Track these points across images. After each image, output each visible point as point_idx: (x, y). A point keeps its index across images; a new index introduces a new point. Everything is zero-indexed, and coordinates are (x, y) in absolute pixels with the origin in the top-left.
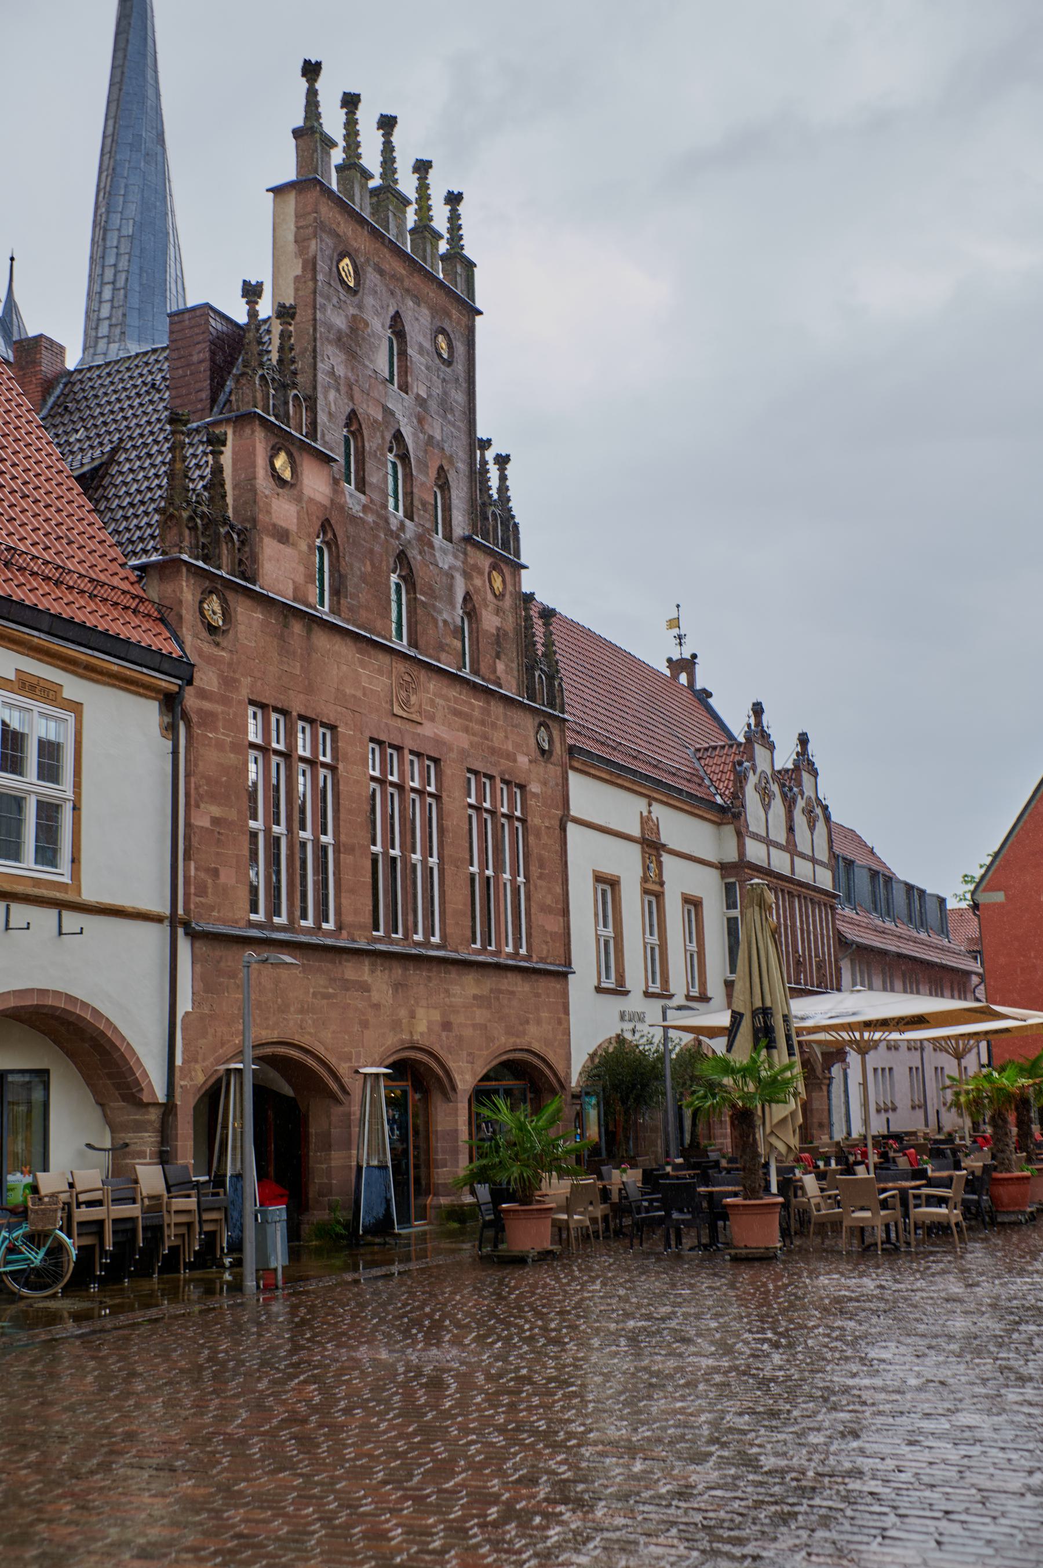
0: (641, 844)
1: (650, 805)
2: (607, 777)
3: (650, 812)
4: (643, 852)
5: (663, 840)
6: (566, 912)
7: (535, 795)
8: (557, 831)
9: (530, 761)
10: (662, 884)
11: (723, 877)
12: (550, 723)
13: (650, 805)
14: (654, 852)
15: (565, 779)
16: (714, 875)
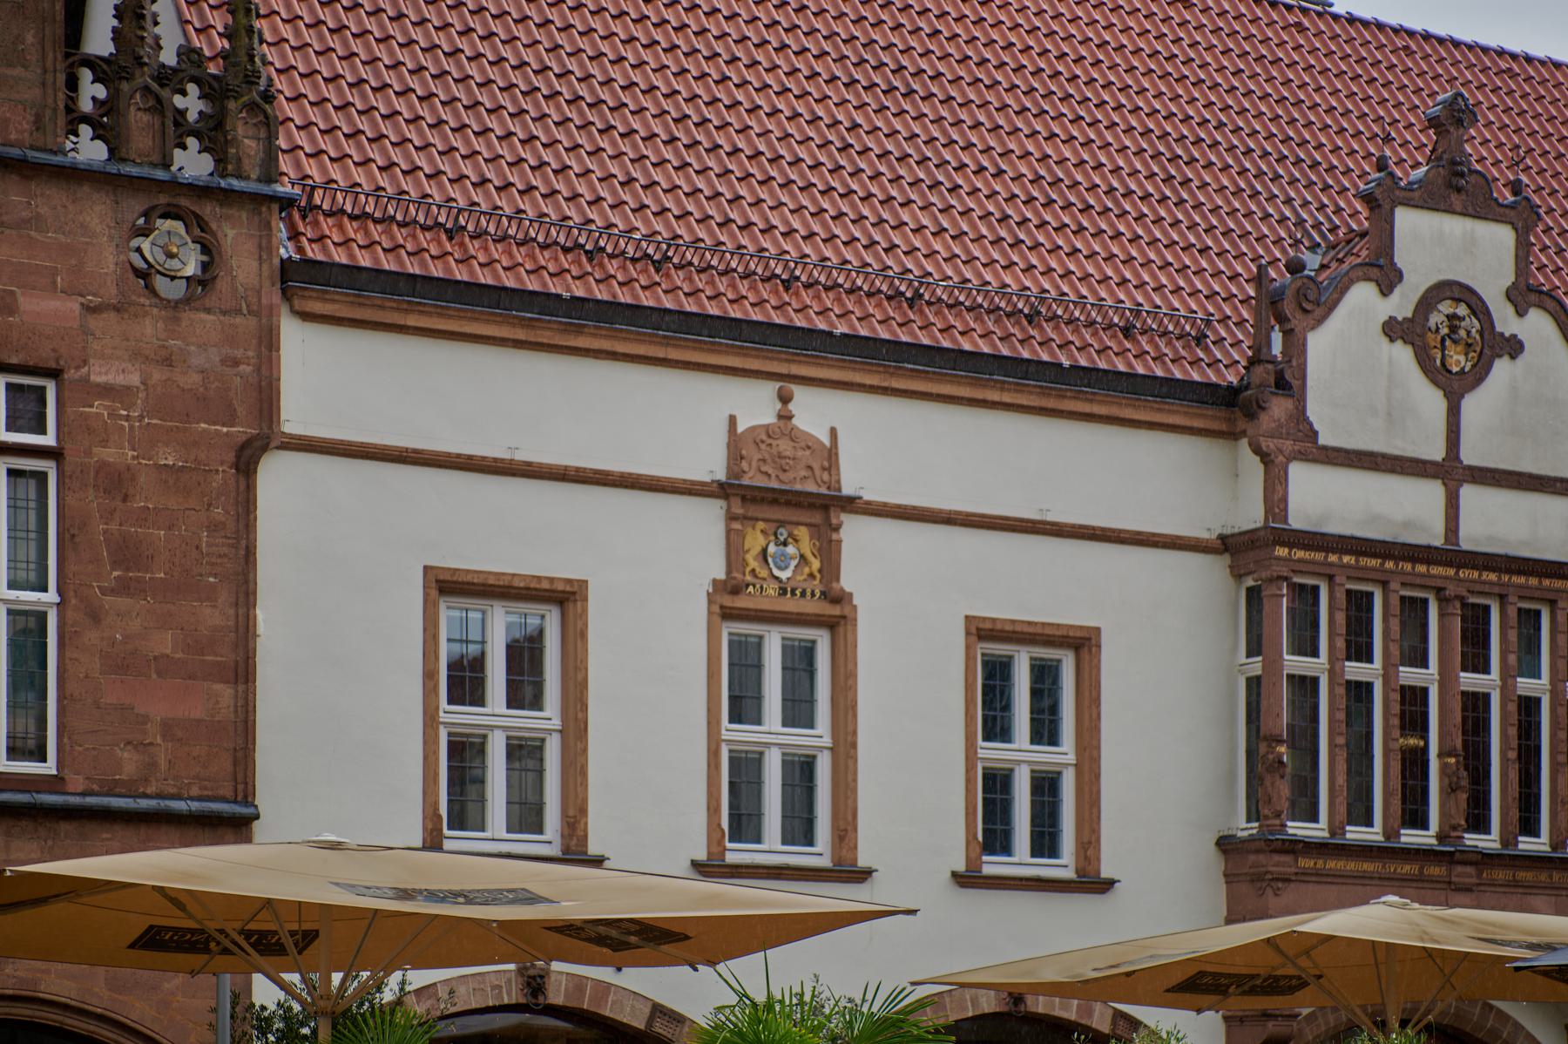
0: (726, 497)
1: (785, 399)
2: (521, 334)
3: (785, 417)
4: (731, 517)
5: (847, 490)
6: (243, 673)
7: (107, 391)
8: (223, 475)
9: (89, 309)
10: (841, 598)
11: (1237, 574)
12: (208, 210)
13: (785, 399)
14: (817, 518)
15: (269, 342)
16: (1210, 572)
